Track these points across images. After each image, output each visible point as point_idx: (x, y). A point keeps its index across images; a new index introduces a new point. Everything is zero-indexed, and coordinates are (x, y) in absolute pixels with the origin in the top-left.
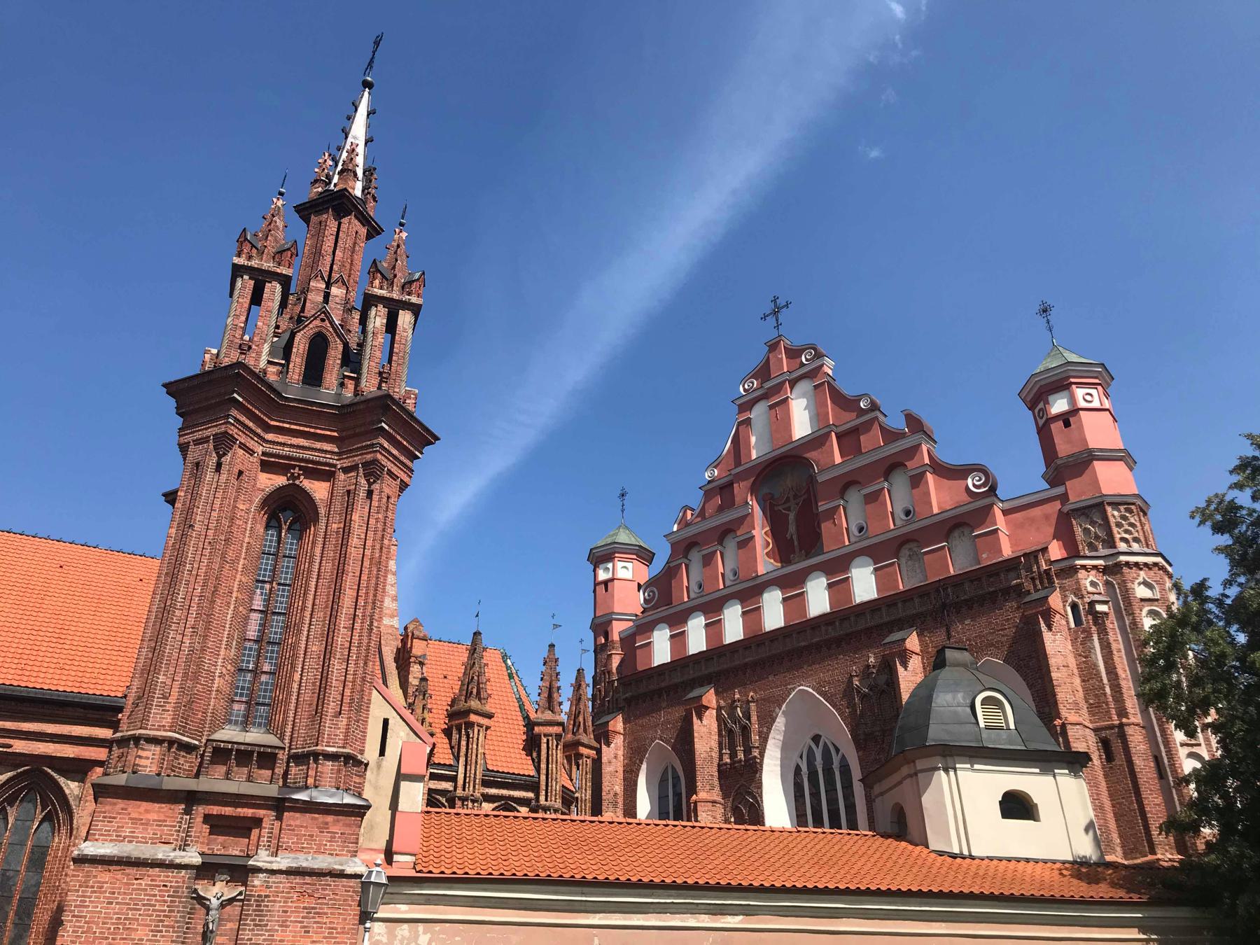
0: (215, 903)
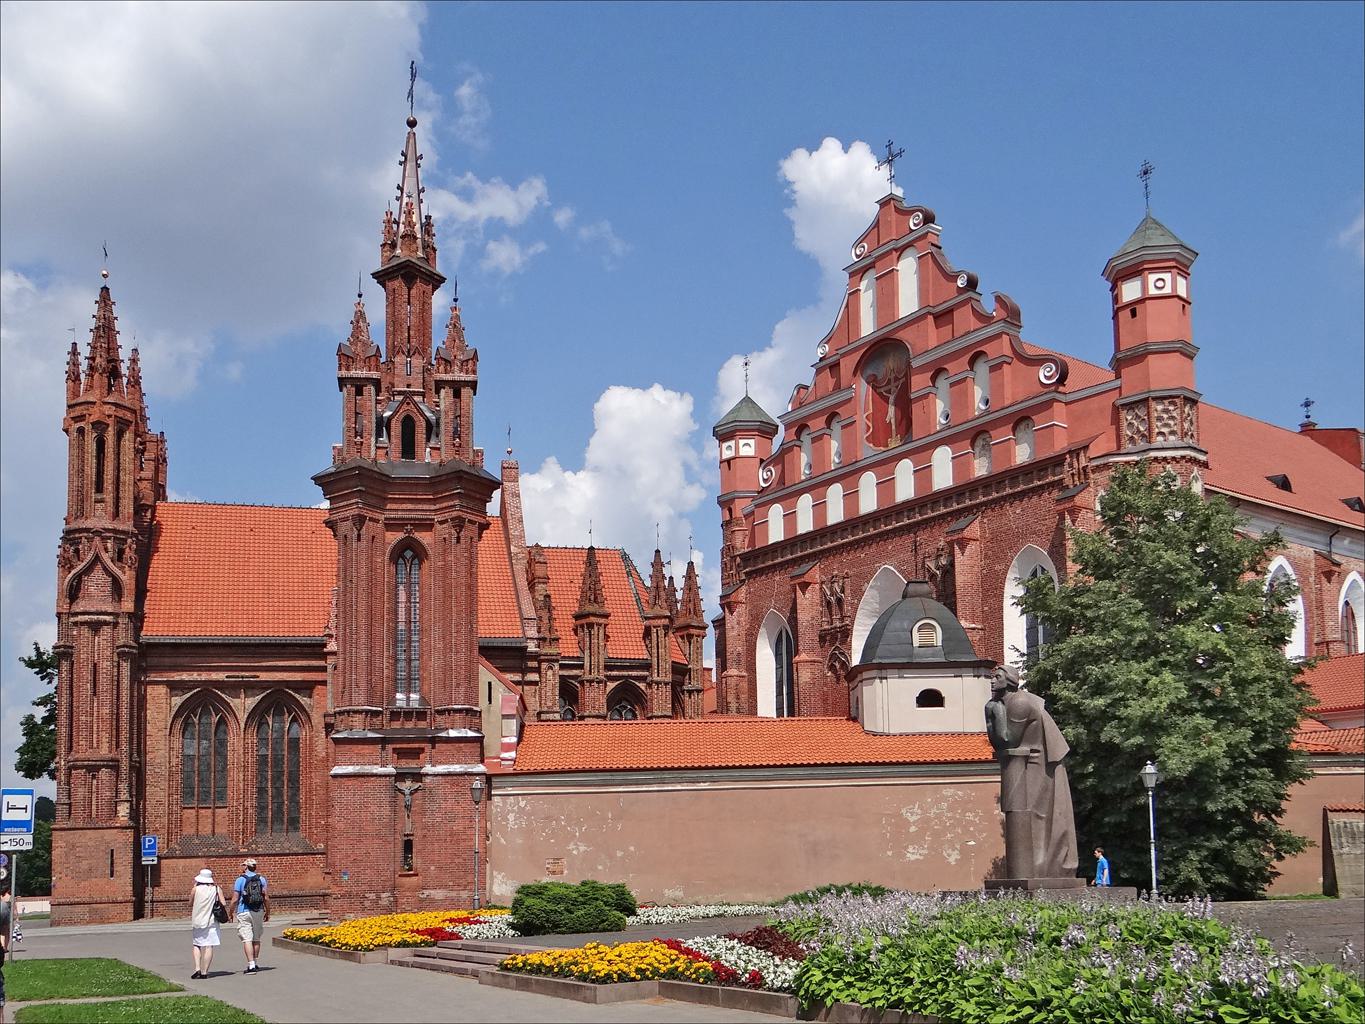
0: (407, 792)
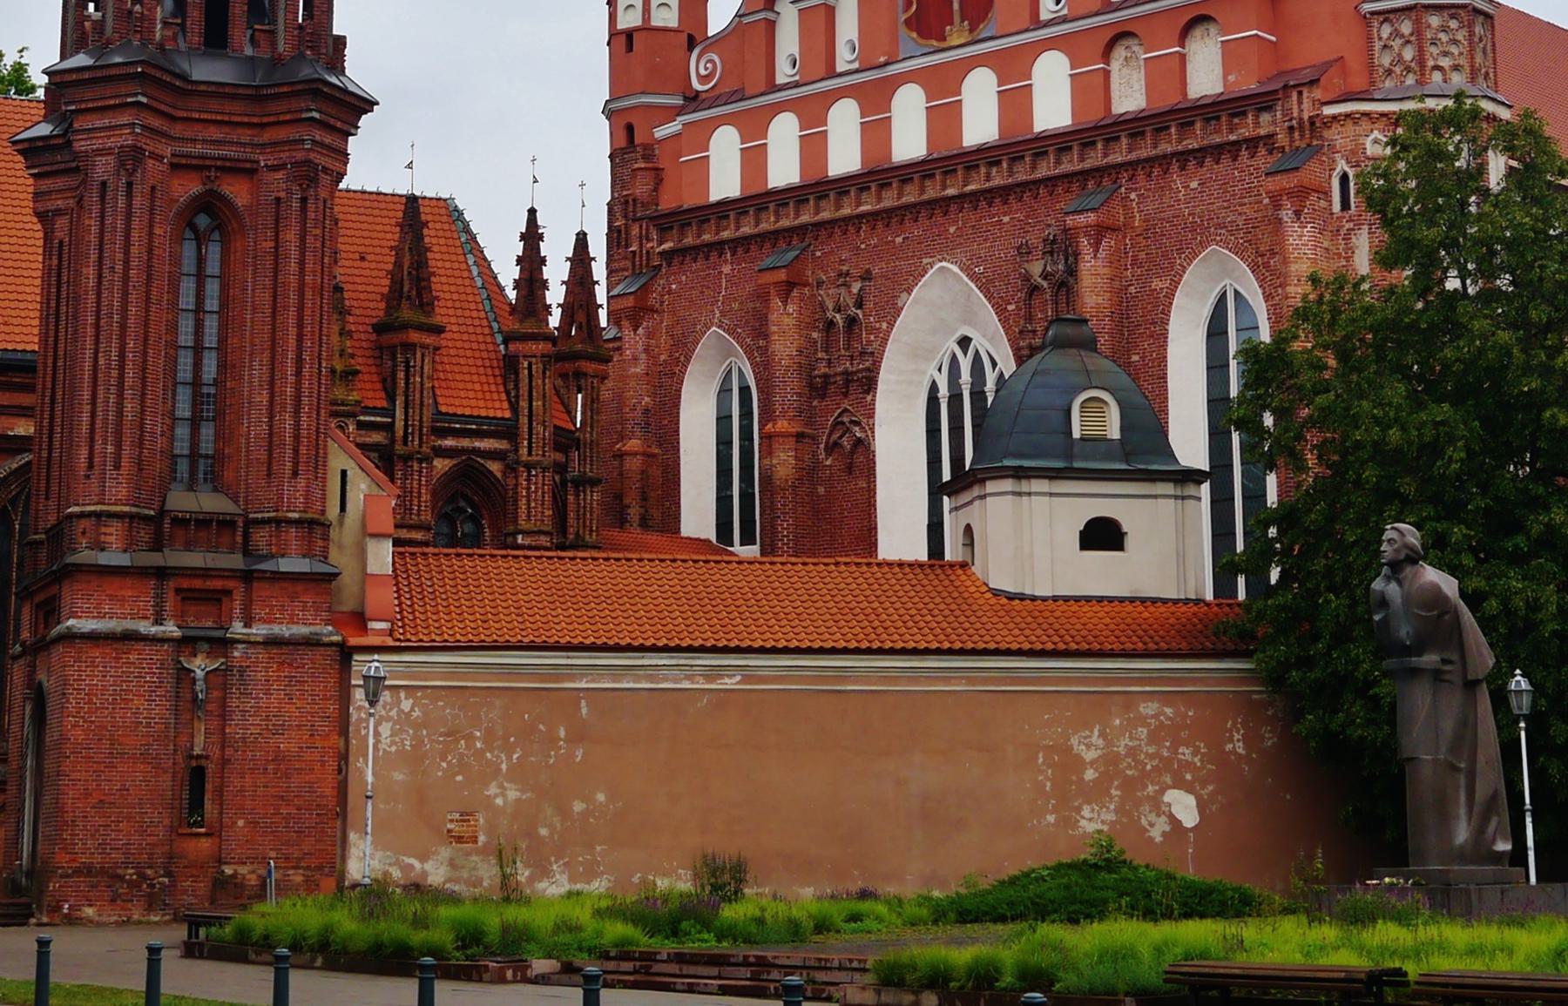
0: (200, 674)
